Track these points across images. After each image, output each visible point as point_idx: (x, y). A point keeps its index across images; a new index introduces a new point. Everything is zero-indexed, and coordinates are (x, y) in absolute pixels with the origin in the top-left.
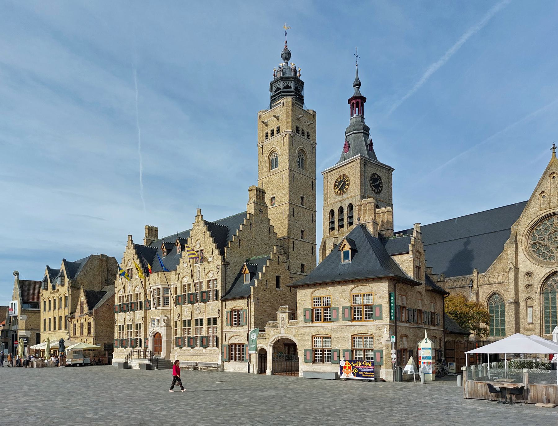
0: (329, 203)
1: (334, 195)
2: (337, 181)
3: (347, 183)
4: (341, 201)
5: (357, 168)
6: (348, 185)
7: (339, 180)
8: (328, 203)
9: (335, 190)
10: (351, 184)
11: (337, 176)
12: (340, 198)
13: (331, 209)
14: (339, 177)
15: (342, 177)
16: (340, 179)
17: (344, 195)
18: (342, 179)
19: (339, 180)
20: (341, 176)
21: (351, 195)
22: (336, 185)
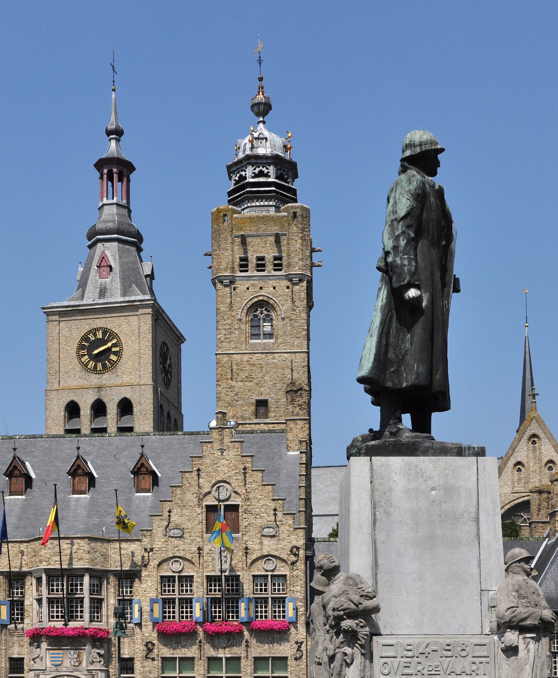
0: (61, 383)
1: (78, 367)
2: (85, 338)
3: (114, 349)
4: (100, 388)
5: (142, 324)
6: (116, 353)
7: (92, 338)
8: (61, 385)
9: (80, 356)
10: (125, 354)
11: (88, 328)
12: (94, 379)
13: (70, 399)
14: (94, 331)
15: (101, 332)
16: (95, 335)
17: (106, 376)
18: (100, 335)
19: (92, 338)
20: (97, 329)
21: (126, 379)
22: (81, 347)
